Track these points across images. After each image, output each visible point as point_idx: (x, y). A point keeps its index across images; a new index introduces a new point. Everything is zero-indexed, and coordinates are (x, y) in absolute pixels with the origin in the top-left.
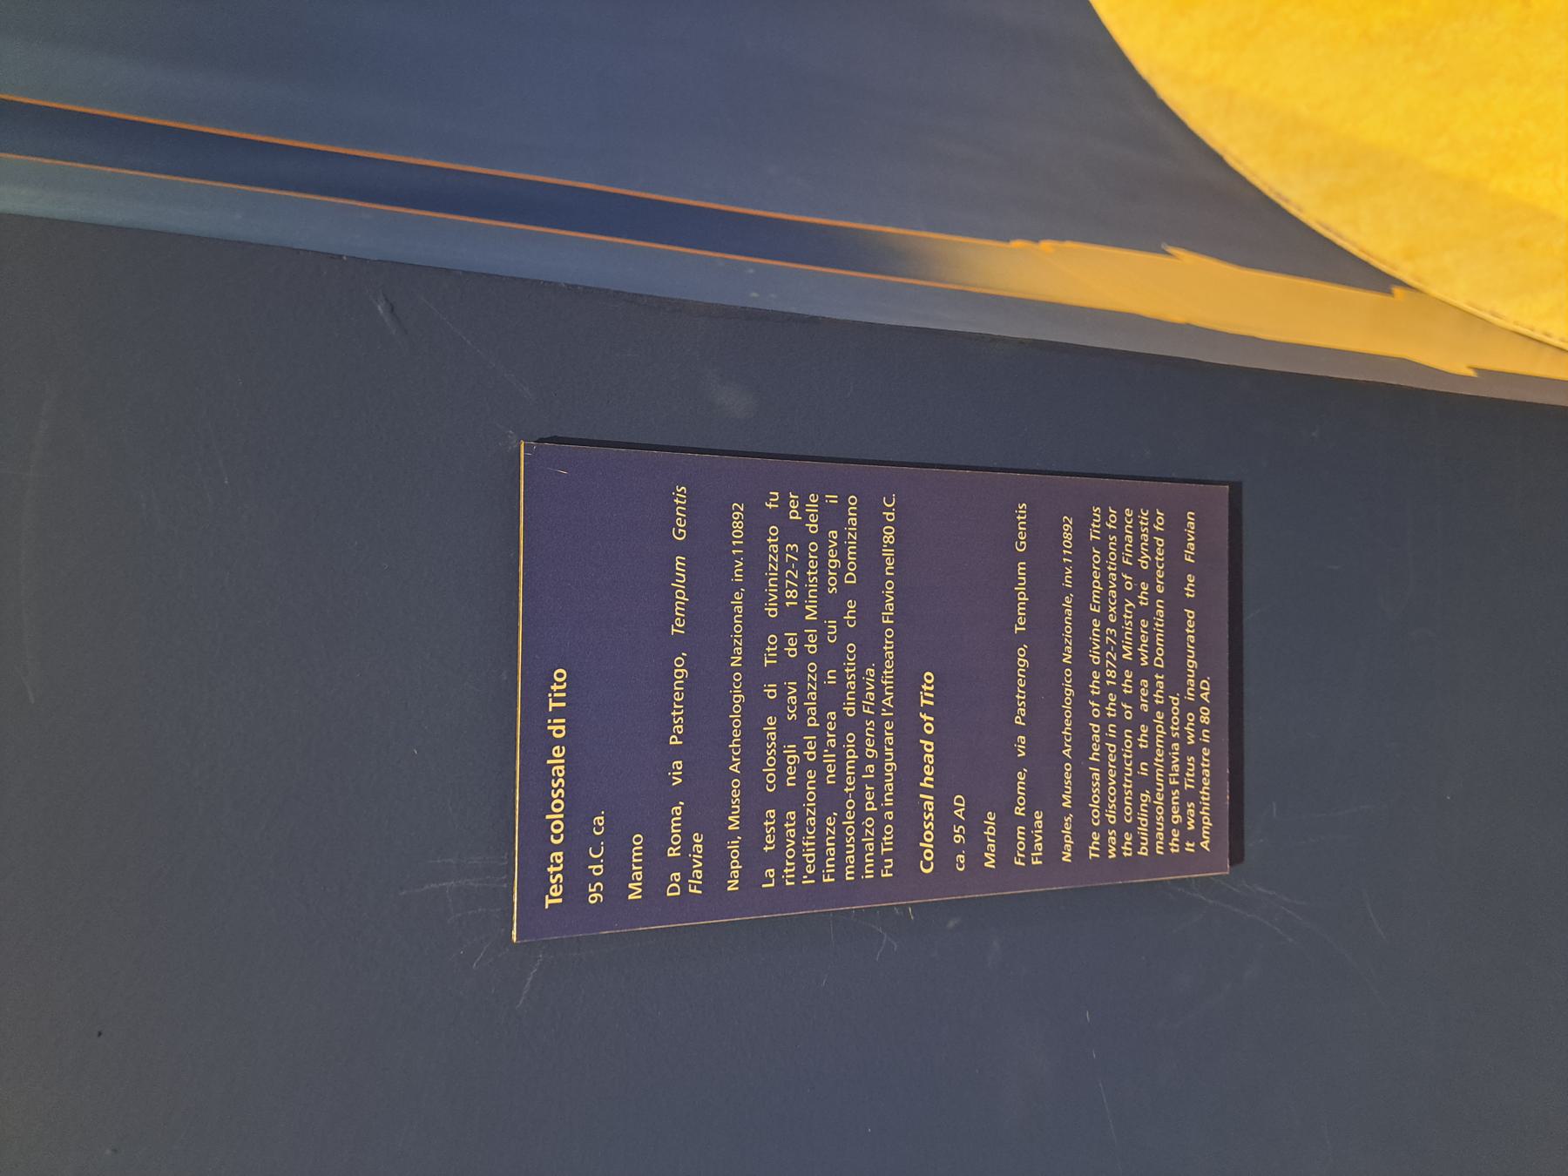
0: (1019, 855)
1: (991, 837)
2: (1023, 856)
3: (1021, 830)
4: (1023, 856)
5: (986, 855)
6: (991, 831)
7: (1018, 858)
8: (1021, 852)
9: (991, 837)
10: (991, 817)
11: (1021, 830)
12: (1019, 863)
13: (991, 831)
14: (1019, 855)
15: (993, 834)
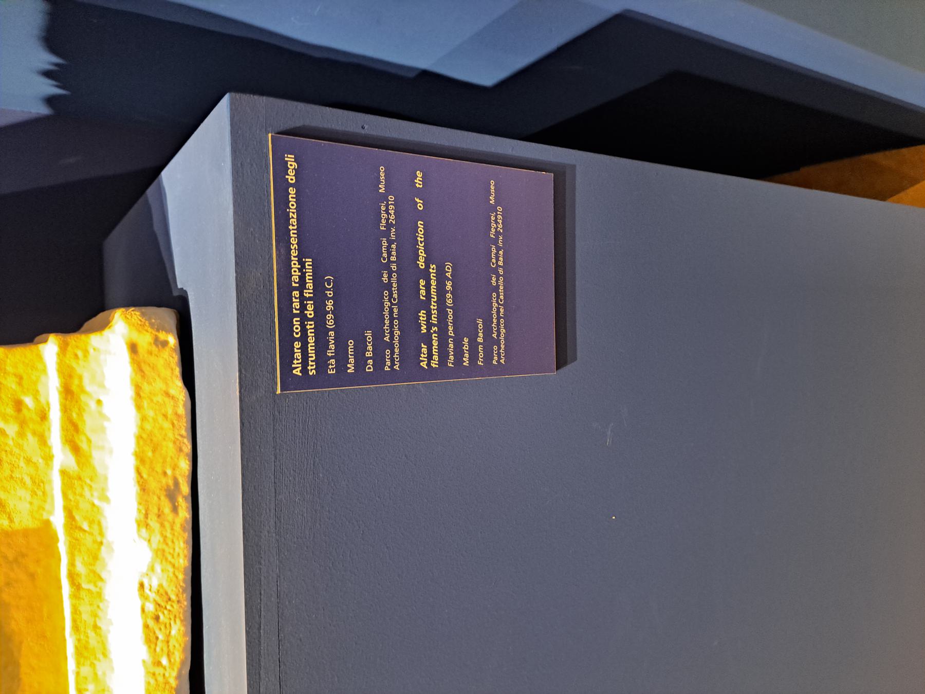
0: (480, 359)
1: (466, 350)
2: (482, 360)
3: (481, 347)
4: (482, 360)
5: (464, 359)
6: (466, 347)
7: (480, 361)
8: (481, 358)
9: (466, 350)
10: (466, 340)
11: (481, 347)
12: (481, 364)
13: (466, 347)
14: (480, 359)
15: (467, 349)
